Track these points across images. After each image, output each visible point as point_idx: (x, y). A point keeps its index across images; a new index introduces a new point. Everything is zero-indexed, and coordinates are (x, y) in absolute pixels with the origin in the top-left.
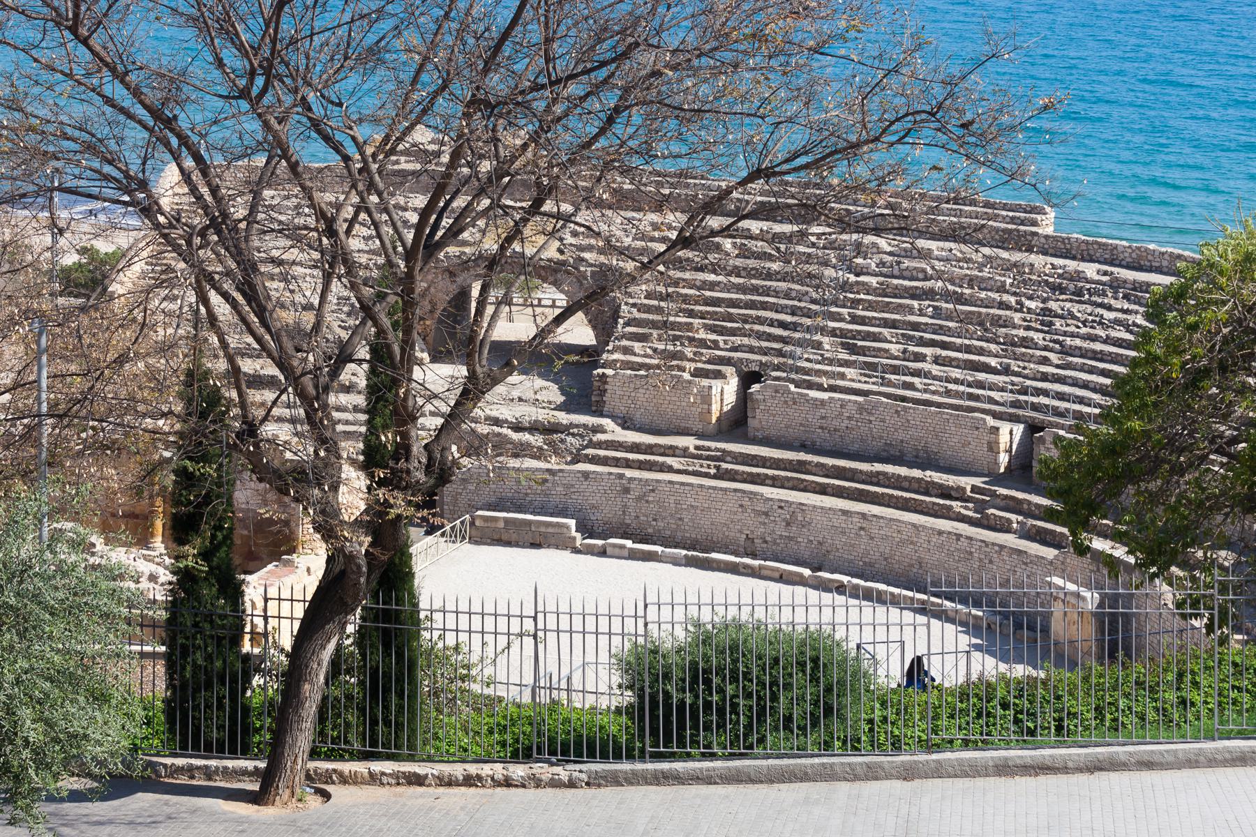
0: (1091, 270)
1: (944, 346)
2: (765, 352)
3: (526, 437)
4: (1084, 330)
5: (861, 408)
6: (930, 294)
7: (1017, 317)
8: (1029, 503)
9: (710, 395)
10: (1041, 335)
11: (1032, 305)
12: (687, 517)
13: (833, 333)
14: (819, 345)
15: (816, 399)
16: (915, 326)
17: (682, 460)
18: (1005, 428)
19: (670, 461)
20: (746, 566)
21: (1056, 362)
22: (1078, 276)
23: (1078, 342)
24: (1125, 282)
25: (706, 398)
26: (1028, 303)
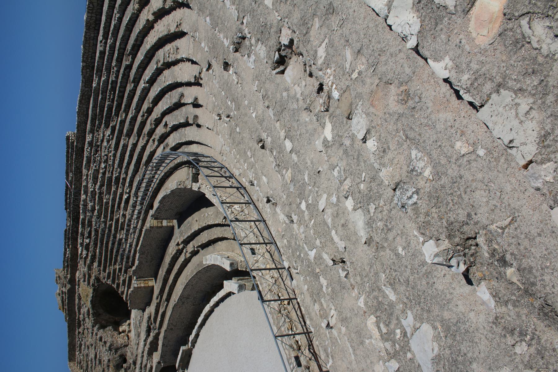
0: (88, 138)
5: (142, 253)
6: (101, 193)
9: (138, 288)
10: (114, 173)
11: (103, 165)
14: (121, 240)
15: (139, 263)
16: (113, 206)
17: (161, 307)
19: (161, 311)
21: (125, 176)
23: (117, 162)
26: (103, 165)
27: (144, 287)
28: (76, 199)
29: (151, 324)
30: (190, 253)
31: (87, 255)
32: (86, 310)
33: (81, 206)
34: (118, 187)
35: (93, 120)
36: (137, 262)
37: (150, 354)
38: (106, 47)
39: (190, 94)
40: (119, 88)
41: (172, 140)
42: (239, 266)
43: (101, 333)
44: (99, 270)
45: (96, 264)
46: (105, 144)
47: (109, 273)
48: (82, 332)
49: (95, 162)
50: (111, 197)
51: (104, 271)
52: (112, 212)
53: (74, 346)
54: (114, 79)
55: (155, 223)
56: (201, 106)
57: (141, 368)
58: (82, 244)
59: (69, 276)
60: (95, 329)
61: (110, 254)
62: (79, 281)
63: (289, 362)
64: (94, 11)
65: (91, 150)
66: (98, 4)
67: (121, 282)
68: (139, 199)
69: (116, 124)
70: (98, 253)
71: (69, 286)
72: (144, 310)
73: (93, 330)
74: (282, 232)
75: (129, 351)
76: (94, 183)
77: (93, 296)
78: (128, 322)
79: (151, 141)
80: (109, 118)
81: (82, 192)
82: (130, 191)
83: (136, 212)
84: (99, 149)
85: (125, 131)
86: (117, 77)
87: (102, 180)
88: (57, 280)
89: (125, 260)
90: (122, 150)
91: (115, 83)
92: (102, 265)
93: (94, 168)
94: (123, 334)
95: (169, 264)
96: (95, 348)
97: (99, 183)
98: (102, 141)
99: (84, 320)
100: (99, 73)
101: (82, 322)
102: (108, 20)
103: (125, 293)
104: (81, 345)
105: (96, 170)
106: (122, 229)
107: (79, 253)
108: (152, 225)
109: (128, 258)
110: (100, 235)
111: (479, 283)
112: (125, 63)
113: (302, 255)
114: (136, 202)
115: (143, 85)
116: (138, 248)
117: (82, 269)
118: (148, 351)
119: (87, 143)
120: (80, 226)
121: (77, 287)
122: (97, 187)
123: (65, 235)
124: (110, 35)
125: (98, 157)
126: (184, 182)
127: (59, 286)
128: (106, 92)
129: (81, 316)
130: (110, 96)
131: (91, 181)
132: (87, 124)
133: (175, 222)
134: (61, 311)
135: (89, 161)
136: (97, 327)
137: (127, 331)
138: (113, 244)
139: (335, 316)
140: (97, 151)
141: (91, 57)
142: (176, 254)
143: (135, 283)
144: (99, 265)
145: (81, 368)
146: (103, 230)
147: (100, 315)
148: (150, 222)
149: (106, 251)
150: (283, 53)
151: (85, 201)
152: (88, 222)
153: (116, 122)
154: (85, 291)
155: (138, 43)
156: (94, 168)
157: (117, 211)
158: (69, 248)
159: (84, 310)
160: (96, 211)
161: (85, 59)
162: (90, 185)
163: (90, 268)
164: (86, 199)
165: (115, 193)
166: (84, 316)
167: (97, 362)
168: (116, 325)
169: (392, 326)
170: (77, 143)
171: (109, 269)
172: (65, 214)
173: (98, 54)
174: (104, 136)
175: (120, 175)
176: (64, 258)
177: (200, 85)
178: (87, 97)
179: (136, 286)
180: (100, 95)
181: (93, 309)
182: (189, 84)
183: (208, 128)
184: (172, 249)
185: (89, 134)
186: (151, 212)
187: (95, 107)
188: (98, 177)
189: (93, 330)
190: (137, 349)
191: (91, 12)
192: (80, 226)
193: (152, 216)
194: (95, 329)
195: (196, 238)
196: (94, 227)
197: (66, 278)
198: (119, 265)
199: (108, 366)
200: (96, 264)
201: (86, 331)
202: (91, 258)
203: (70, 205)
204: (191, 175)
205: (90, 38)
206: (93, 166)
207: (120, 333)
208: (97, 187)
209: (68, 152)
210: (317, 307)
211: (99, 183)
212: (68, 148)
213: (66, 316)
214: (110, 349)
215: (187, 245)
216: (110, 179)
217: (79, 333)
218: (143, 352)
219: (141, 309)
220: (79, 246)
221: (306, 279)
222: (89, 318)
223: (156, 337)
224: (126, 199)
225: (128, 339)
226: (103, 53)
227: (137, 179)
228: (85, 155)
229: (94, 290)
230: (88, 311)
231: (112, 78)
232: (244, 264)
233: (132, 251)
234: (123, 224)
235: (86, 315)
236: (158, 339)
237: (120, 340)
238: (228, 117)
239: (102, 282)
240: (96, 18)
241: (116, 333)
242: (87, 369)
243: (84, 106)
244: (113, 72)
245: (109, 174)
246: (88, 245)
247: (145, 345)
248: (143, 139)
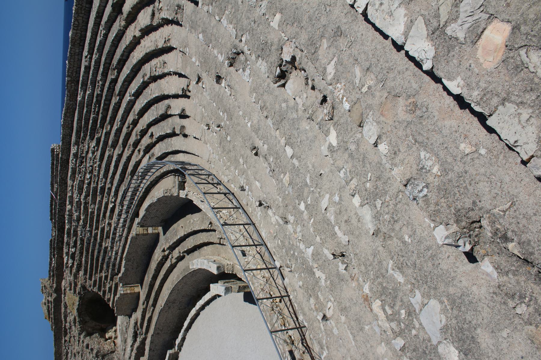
0: (73, 150)
5: (127, 260)
6: (86, 203)
7: (92, 186)
9: (124, 294)
10: (99, 183)
11: (88, 176)
14: (106, 248)
15: (125, 270)
16: (98, 215)
19: (147, 316)
23: (102, 173)
24: (76, 141)
26: (88, 176)
27: (130, 293)
28: (61, 210)
29: (138, 329)
30: (176, 259)
31: (73, 264)
32: (72, 318)
33: (66, 217)
34: (103, 197)
36: (123, 269)
38: (91, 62)
39: (177, 106)
40: (105, 100)
41: (158, 150)
42: (225, 269)
43: (87, 340)
44: (85, 279)
45: (81, 273)
46: (90, 155)
47: (95, 281)
48: (68, 340)
49: (80, 173)
50: (97, 206)
51: (90, 279)
52: (98, 221)
53: (61, 354)
54: (99, 93)
55: (141, 230)
56: (188, 117)
58: (67, 254)
59: (55, 285)
60: (82, 336)
61: (96, 263)
62: (65, 290)
63: (283, 356)
64: (79, 28)
65: (76, 161)
66: (83, 21)
67: (107, 289)
68: (125, 207)
69: (101, 136)
70: (83, 262)
71: (54, 295)
72: (130, 316)
73: (79, 338)
74: (274, 233)
75: (116, 357)
76: (79, 193)
77: (79, 304)
78: (114, 328)
79: (136, 151)
80: (94, 130)
81: (68, 203)
82: (115, 201)
83: (122, 220)
84: (84, 160)
85: (110, 142)
86: (102, 91)
87: (87, 190)
88: (42, 290)
89: (111, 267)
90: (107, 160)
91: (100, 96)
92: (88, 273)
93: (79, 179)
94: (109, 341)
95: (155, 270)
96: (82, 356)
97: (84, 194)
98: (87, 152)
99: (70, 328)
100: (84, 87)
101: (68, 331)
102: (94, 36)
103: (111, 300)
105: (82, 181)
106: (108, 237)
107: (65, 262)
108: (138, 233)
109: (114, 265)
110: (85, 244)
111: (483, 259)
112: (110, 77)
113: (296, 254)
114: (122, 211)
115: (129, 98)
116: (124, 256)
117: (68, 277)
118: (135, 356)
119: (71, 154)
120: (66, 236)
121: (63, 296)
122: (82, 197)
123: (51, 245)
124: (96, 51)
125: (83, 168)
126: (170, 190)
127: (44, 295)
128: (92, 106)
129: (68, 324)
130: (95, 109)
131: (76, 192)
132: (72, 136)
133: (160, 229)
134: (47, 320)
136: (83, 334)
137: (113, 337)
138: (99, 252)
139: (332, 308)
140: (82, 162)
141: (76, 72)
142: (162, 260)
143: (121, 290)
144: (85, 274)
146: (89, 240)
147: (86, 322)
148: (136, 230)
150: (284, 69)
151: (70, 211)
152: (74, 231)
154: (71, 300)
155: (124, 58)
156: (79, 179)
157: (103, 220)
158: (54, 258)
159: (70, 318)
160: (82, 221)
161: (70, 74)
163: (76, 276)
164: (71, 209)
165: (101, 202)
166: (70, 324)
168: (102, 332)
169: (397, 308)
170: (62, 155)
171: (95, 277)
172: (50, 225)
173: (83, 69)
174: (89, 147)
175: (105, 186)
176: (50, 268)
177: (189, 97)
178: (71, 110)
179: (122, 292)
180: (85, 108)
181: (79, 317)
182: (176, 96)
183: (195, 138)
184: (157, 255)
185: (74, 146)
186: (137, 220)
187: (80, 119)
188: (83, 187)
189: (79, 338)
190: (124, 354)
191: (76, 28)
192: (66, 236)
193: (138, 224)
194: (82, 336)
195: (182, 244)
196: (79, 236)
197: (52, 287)
198: (105, 273)
200: (81, 273)
201: (72, 339)
202: (77, 267)
203: (55, 216)
204: (177, 183)
205: (75, 54)
206: (78, 177)
207: (106, 340)
208: (82, 197)
209: (53, 164)
210: (312, 301)
211: (84, 194)
212: (53, 160)
213: (52, 325)
214: (97, 356)
215: (172, 251)
216: (95, 189)
217: (65, 341)
219: (127, 315)
220: (64, 255)
221: (301, 276)
222: (75, 326)
224: (111, 208)
225: (115, 345)
226: (88, 68)
227: (123, 188)
228: (70, 167)
229: (80, 298)
230: (75, 319)
231: (97, 91)
232: (230, 267)
233: (118, 259)
234: (108, 232)
235: (72, 323)
236: (145, 344)
237: (107, 347)
238: (219, 126)
240: (81, 34)
241: (102, 340)
243: (69, 119)
244: (98, 86)
245: (94, 184)
246: (74, 254)
247: (132, 350)
248: (128, 150)
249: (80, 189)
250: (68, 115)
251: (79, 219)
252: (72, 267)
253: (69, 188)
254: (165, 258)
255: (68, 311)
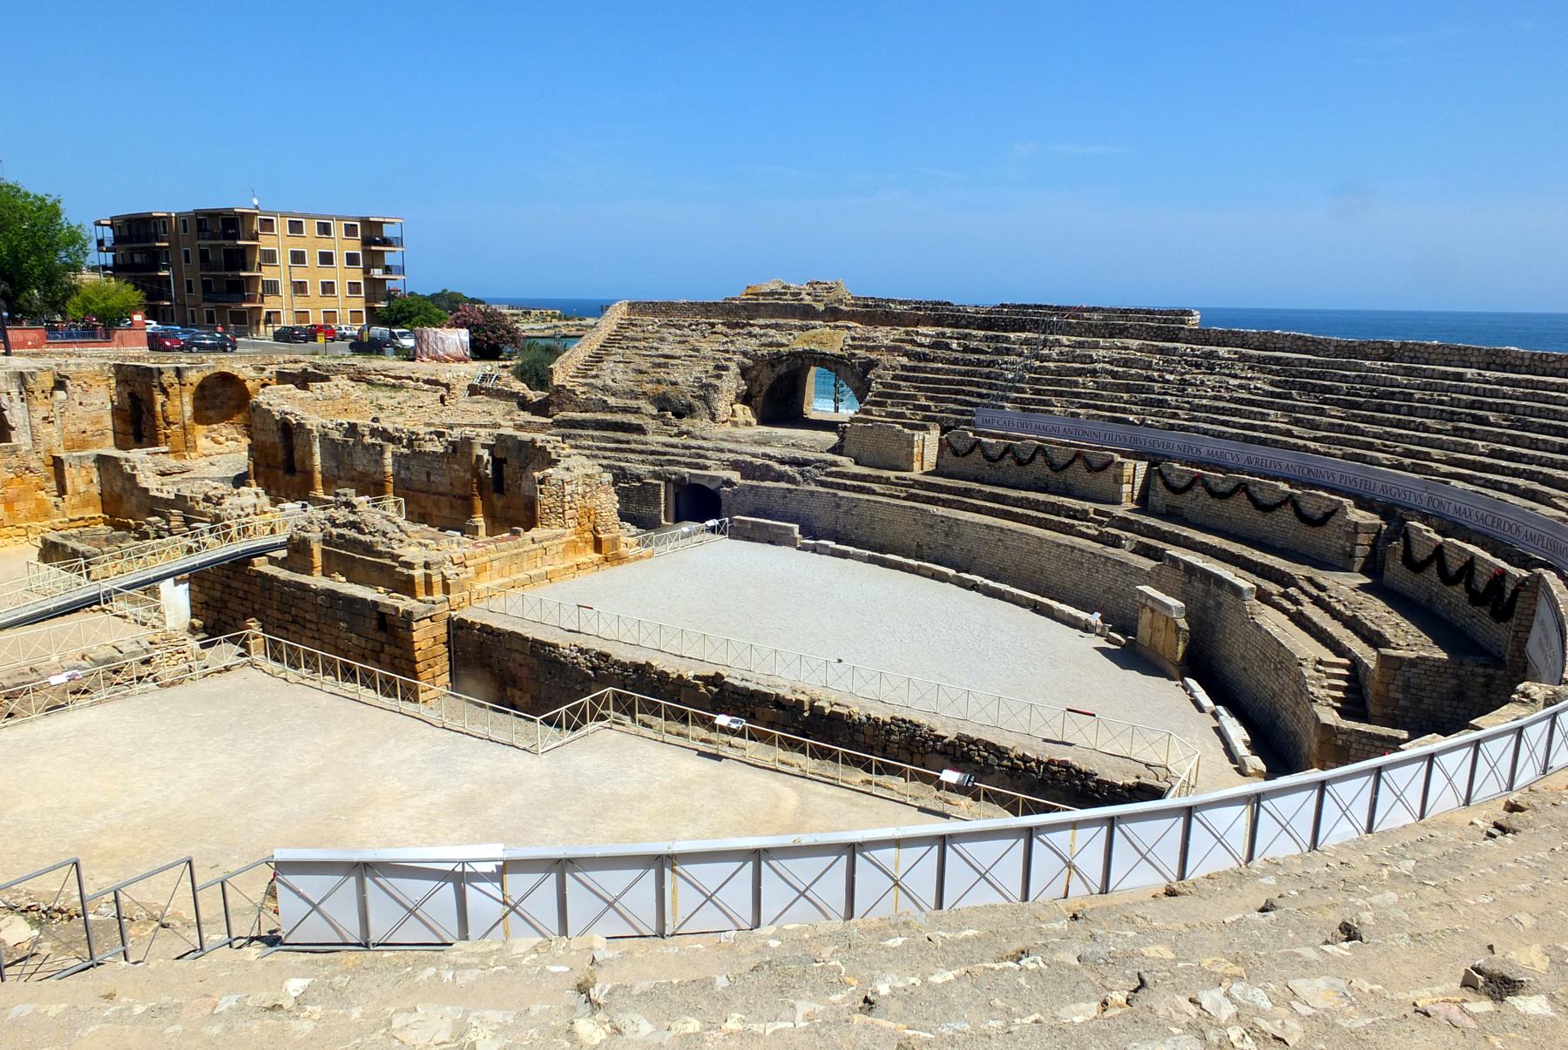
1: (1096, 407)
2: (962, 413)
3: (787, 468)
4: (1211, 393)
6: (1094, 372)
7: (1156, 386)
8: (1139, 523)
11: (1171, 377)
12: (877, 527)
13: (1014, 401)
16: (1077, 395)
18: (1129, 464)
20: (909, 566)
22: (1211, 355)
23: (1204, 402)
25: (911, 444)
26: (1168, 377)
31: (922, 345)
35: (1278, 361)
37: (735, 465)
43: (733, 366)
44: (895, 369)
45: (904, 360)
47: (899, 388)
57: (685, 447)
62: (849, 328)
70: (931, 365)
71: (821, 307)
78: (754, 421)
91: (1409, 397)
98: (1235, 376)
99: (750, 334)
104: (680, 327)
112: (1492, 416)
122: (1108, 366)
129: (756, 330)
134: (743, 290)
135: (1161, 351)
140: (1198, 366)
144: (904, 367)
145: (621, 326)
147: (773, 366)
149: (949, 382)
153: (1299, 400)
154: (834, 339)
162: (1102, 352)
163: (890, 350)
164: (1061, 345)
167: (657, 360)
168: (745, 399)
175: (1170, 407)
196: (999, 359)
199: (659, 382)
200: (904, 360)
206: (1156, 359)
208: (1108, 366)
214: (704, 386)
216: (1150, 390)
217: (713, 325)
218: (730, 451)
223: (780, 477)
226: (1459, 377)
230: (783, 345)
237: (722, 406)
239: (866, 372)
241: (733, 397)
242: (626, 338)
246: (947, 347)
247: (754, 455)
249: (1126, 363)
250: (1300, 342)
251: (1044, 359)
252: (913, 342)
253: (1118, 342)
254: (1082, 516)
255: (796, 333)
